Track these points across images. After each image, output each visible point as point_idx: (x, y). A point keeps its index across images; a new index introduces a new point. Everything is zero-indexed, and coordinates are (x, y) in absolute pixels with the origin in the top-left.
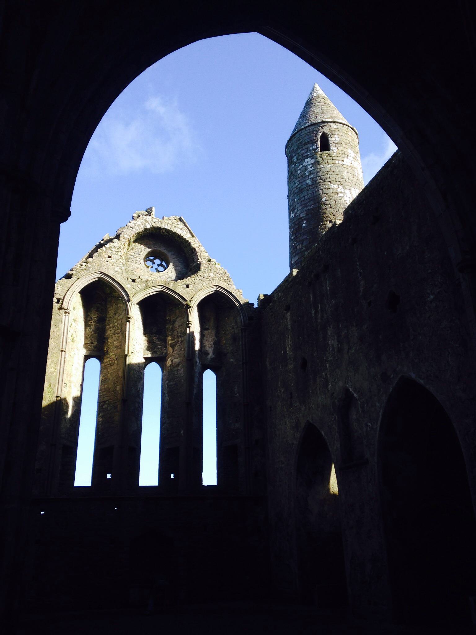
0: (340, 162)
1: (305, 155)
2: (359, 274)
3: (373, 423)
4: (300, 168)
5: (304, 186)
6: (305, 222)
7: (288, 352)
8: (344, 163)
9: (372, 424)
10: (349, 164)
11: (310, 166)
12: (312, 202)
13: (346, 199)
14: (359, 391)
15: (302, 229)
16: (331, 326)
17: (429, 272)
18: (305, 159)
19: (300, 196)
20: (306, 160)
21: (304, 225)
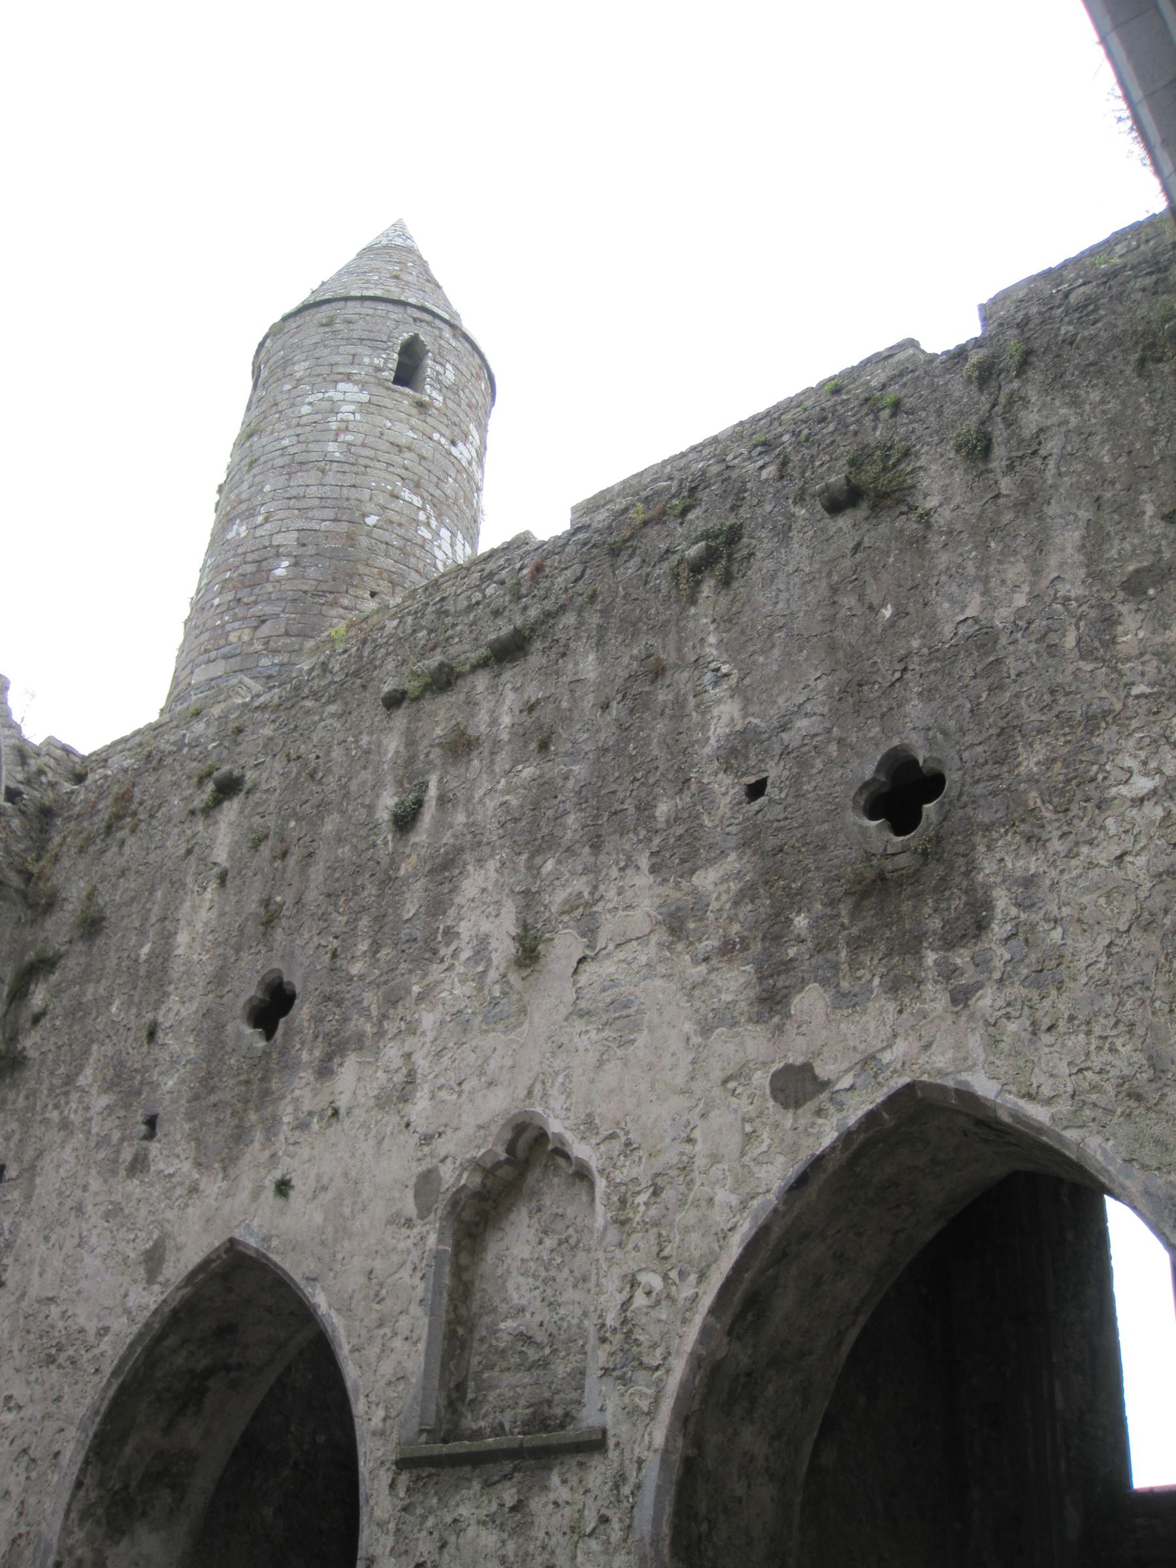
0: (443, 441)
1: (342, 370)
2: (709, 677)
3: (673, 1274)
4: (310, 399)
5: (314, 456)
6: (286, 563)
7: (179, 951)
8: (453, 450)
9: (665, 1277)
10: (465, 464)
11: (352, 408)
12: (330, 513)
13: (437, 552)
14: (613, 1136)
15: (268, 581)
16: (492, 865)
17: (1135, 691)
18: (336, 382)
19: (289, 480)
20: (341, 386)
21: (280, 572)
